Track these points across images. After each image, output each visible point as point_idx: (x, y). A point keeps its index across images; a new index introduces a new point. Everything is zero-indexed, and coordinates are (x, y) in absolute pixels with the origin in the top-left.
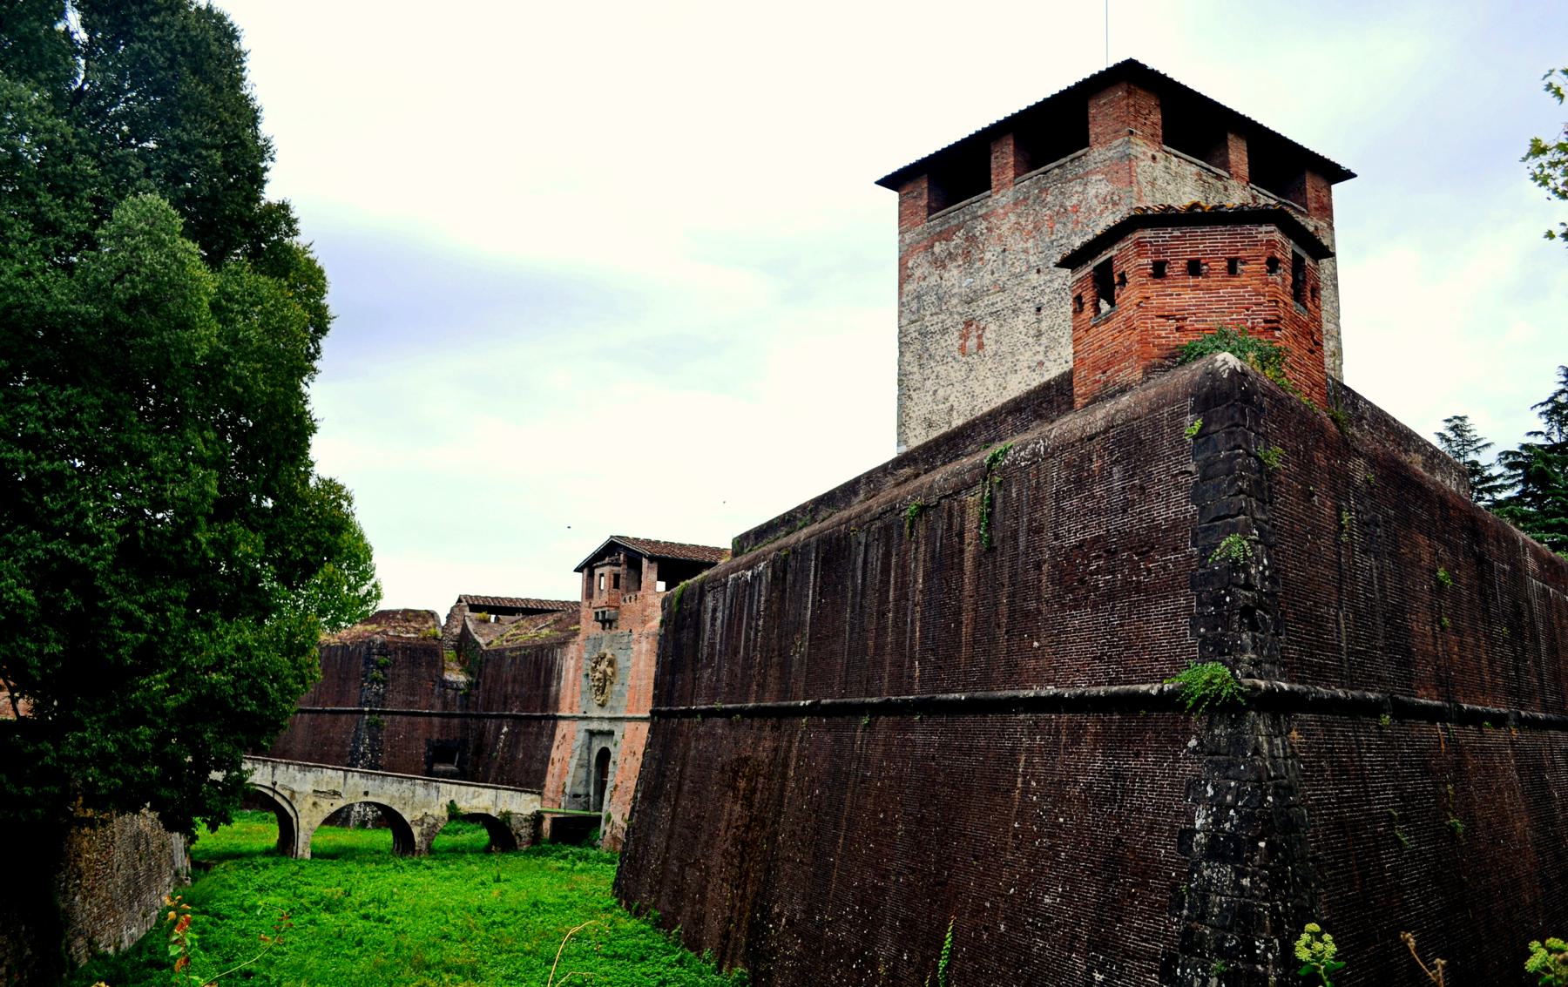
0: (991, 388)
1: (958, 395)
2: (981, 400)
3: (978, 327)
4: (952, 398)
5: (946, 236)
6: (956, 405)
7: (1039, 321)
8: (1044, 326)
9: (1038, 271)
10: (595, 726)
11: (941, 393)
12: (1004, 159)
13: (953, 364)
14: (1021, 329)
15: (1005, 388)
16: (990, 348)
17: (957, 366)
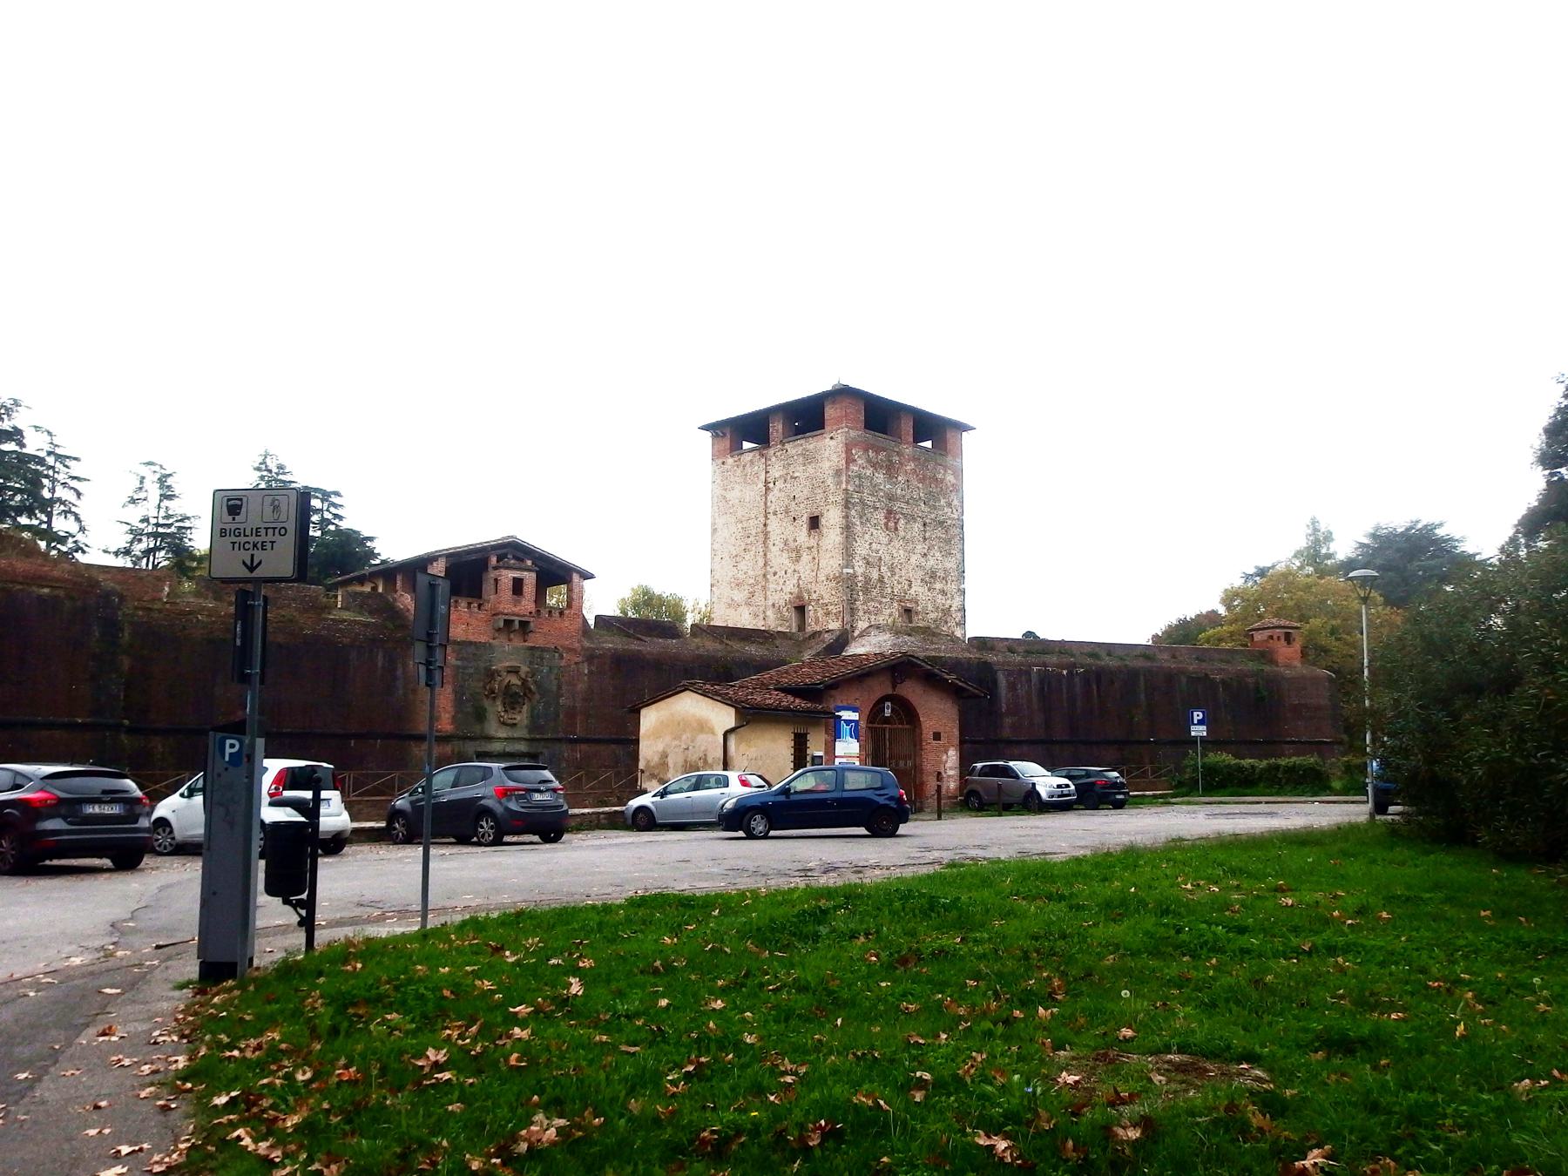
5: (878, 450)
7: (925, 531)
8: (927, 535)
10: (497, 747)
12: (907, 427)
16: (902, 534)
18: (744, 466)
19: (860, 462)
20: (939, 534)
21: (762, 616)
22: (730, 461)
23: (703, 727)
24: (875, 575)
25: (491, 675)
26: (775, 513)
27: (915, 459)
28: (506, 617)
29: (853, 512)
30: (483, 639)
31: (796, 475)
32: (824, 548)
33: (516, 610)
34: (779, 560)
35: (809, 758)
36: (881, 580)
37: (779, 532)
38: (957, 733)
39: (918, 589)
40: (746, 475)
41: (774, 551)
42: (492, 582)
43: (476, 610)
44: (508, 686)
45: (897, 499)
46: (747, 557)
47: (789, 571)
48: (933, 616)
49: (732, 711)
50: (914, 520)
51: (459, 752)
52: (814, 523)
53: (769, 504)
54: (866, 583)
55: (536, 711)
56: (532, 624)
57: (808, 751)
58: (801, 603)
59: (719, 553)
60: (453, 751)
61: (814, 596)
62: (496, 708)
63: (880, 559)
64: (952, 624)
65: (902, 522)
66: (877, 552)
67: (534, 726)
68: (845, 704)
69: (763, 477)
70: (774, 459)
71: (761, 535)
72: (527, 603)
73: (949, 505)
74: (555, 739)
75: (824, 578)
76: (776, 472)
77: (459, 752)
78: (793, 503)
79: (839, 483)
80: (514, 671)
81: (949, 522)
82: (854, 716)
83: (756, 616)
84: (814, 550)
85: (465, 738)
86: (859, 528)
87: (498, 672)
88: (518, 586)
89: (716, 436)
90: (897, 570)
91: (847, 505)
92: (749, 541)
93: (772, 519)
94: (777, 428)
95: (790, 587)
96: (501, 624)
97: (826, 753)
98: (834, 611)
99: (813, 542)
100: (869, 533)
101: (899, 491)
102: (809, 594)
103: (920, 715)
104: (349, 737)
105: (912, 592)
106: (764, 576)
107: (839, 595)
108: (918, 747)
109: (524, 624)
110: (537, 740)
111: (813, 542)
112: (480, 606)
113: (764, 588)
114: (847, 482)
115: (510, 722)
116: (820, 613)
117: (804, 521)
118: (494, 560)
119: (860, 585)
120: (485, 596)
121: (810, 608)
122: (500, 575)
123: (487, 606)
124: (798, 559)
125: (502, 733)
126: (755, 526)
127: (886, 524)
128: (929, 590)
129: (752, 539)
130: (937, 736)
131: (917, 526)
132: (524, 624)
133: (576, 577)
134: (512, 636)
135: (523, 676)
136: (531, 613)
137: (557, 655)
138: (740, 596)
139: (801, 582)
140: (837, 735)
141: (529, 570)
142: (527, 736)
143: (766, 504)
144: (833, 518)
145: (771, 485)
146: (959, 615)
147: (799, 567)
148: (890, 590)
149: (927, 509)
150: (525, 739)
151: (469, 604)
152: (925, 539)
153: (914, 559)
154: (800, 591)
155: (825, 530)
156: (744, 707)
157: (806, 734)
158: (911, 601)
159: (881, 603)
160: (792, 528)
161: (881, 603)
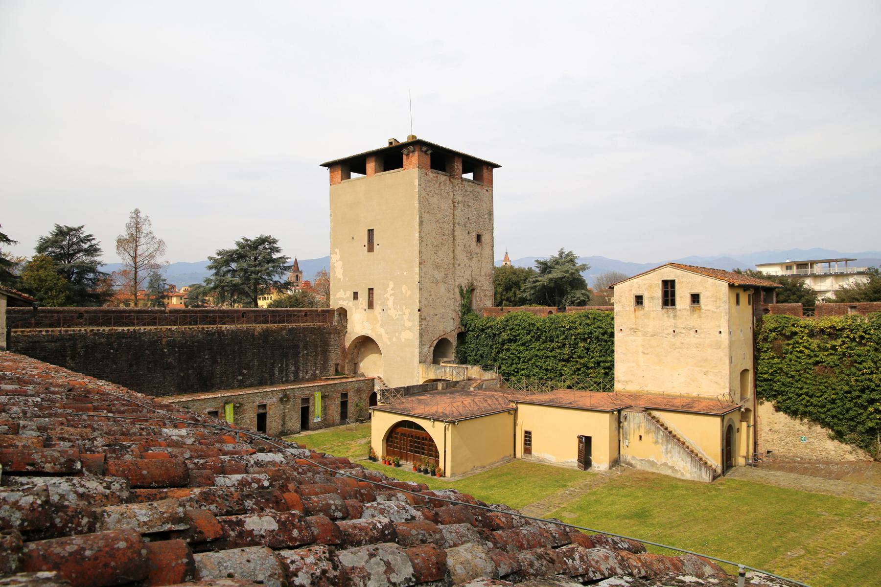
18: (440, 183)
21: (452, 292)
22: (431, 174)
26: (459, 224)
31: (470, 204)
34: (462, 257)
41: (459, 250)
47: (467, 265)
52: (479, 238)
53: (455, 217)
70: (457, 188)
75: (484, 274)
83: (449, 291)
92: (444, 238)
93: (457, 227)
94: (458, 166)
95: (467, 276)
98: (488, 295)
106: (453, 265)
111: (478, 250)
113: (454, 273)
116: (482, 295)
124: (471, 259)
126: (448, 227)
129: (446, 237)
138: (439, 276)
143: (453, 215)
145: (456, 204)
154: (472, 279)
160: (467, 237)
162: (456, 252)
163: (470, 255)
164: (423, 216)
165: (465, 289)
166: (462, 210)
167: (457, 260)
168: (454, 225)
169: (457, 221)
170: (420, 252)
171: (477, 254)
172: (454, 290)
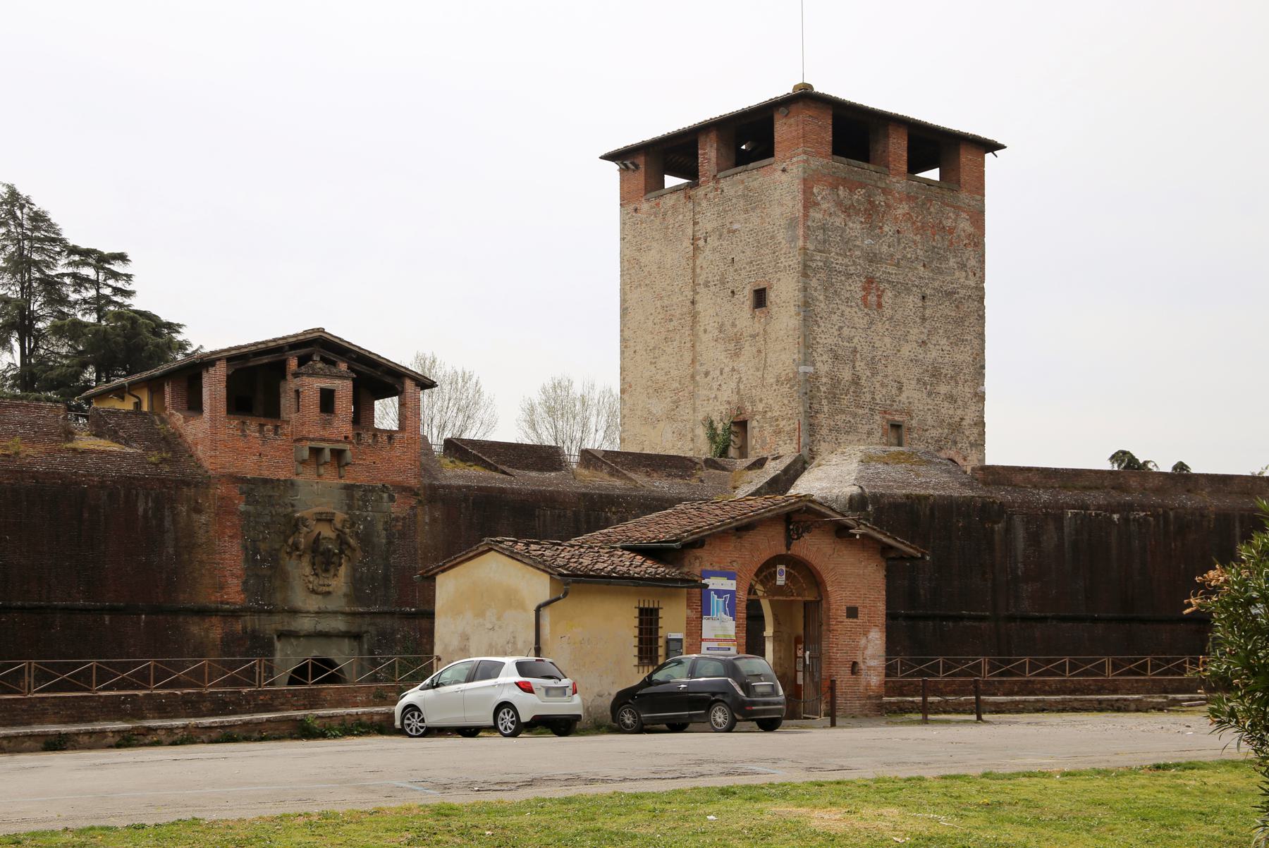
0: (888, 346)
1: (861, 339)
2: (880, 353)
3: (878, 289)
4: (855, 340)
6: (859, 348)
7: (924, 308)
8: (928, 312)
9: (924, 266)
10: (306, 624)
11: (846, 331)
13: (857, 310)
14: (911, 307)
15: (899, 351)
16: (888, 312)
17: (859, 313)
19: (825, 206)
20: (947, 311)
21: (690, 435)
23: (511, 600)
24: (846, 375)
25: (295, 525)
26: (707, 285)
27: (910, 198)
28: (314, 444)
29: (814, 283)
30: (282, 475)
32: (773, 336)
33: (326, 434)
34: (713, 354)
35: (661, 642)
36: (856, 381)
37: (711, 312)
38: (881, 607)
39: (912, 395)
40: (667, 228)
42: (293, 395)
43: (271, 435)
44: (317, 539)
45: (881, 261)
46: (669, 350)
47: (727, 370)
48: (935, 433)
49: (546, 579)
50: (908, 291)
51: (254, 631)
52: (760, 298)
53: (698, 270)
54: (833, 386)
55: (358, 575)
56: (349, 454)
57: (661, 632)
58: (741, 418)
59: (631, 343)
60: (244, 629)
61: (760, 407)
62: (300, 570)
63: (855, 351)
64: (964, 444)
65: (888, 296)
66: (850, 340)
67: (357, 591)
68: (716, 568)
69: (690, 232)
71: (688, 318)
72: (342, 423)
73: (963, 266)
74: (386, 613)
76: (708, 223)
77: (254, 631)
78: (731, 270)
79: (793, 239)
80: (327, 519)
81: (962, 292)
82: (730, 585)
83: (681, 436)
84: (760, 339)
85: (260, 611)
86: (822, 305)
87: (303, 520)
88: (327, 400)
89: (624, 170)
90: (880, 367)
91: (806, 271)
92: (671, 326)
96: (306, 454)
97: (688, 634)
99: (758, 327)
100: (839, 313)
101: (885, 249)
102: (753, 403)
103: (828, 584)
104: (102, 610)
105: (903, 398)
106: (693, 377)
107: (793, 404)
108: (824, 628)
109: (338, 454)
110: (362, 614)
111: (758, 327)
112: (276, 428)
113: (693, 395)
114: (806, 238)
115: (321, 589)
116: (768, 430)
117: (746, 297)
118: (293, 363)
119: (823, 389)
120: (284, 415)
121: (755, 423)
122: (302, 386)
123: (287, 429)
124: (736, 354)
125: (314, 603)
127: (864, 299)
128: (930, 394)
129: (675, 323)
130: (852, 612)
131: (912, 301)
132: (338, 454)
133: (409, 385)
134: (322, 470)
135: (339, 526)
136: (346, 438)
137: (385, 495)
138: (659, 407)
139: (742, 387)
140: (705, 610)
141: (341, 377)
142: (347, 609)
143: (694, 270)
144: (785, 291)
145: (701, 243)
146: (975, 431)
147: (740, 364)
148: (868, 397)
149: (928, 274)
150: (343, 613)
151: (261, 426)
152: (924, 319)
153: (906, 351)
154: (741, 399)
155: (774, 309)
156: (561, 574)
157: (657, 610)
158: (901, 412)
159: (855, 415)
160: (729, 306)
161: (855, 415)
162: (698, 348)
163: (735, 344)
164: (628, 297)
165: (720, 426)
166: (714, 250)
167: (701, 365)
168: (695, 292)
169: (701, 280)
170: (623, 369)
171: (753, 336)
172: (693, 430)
